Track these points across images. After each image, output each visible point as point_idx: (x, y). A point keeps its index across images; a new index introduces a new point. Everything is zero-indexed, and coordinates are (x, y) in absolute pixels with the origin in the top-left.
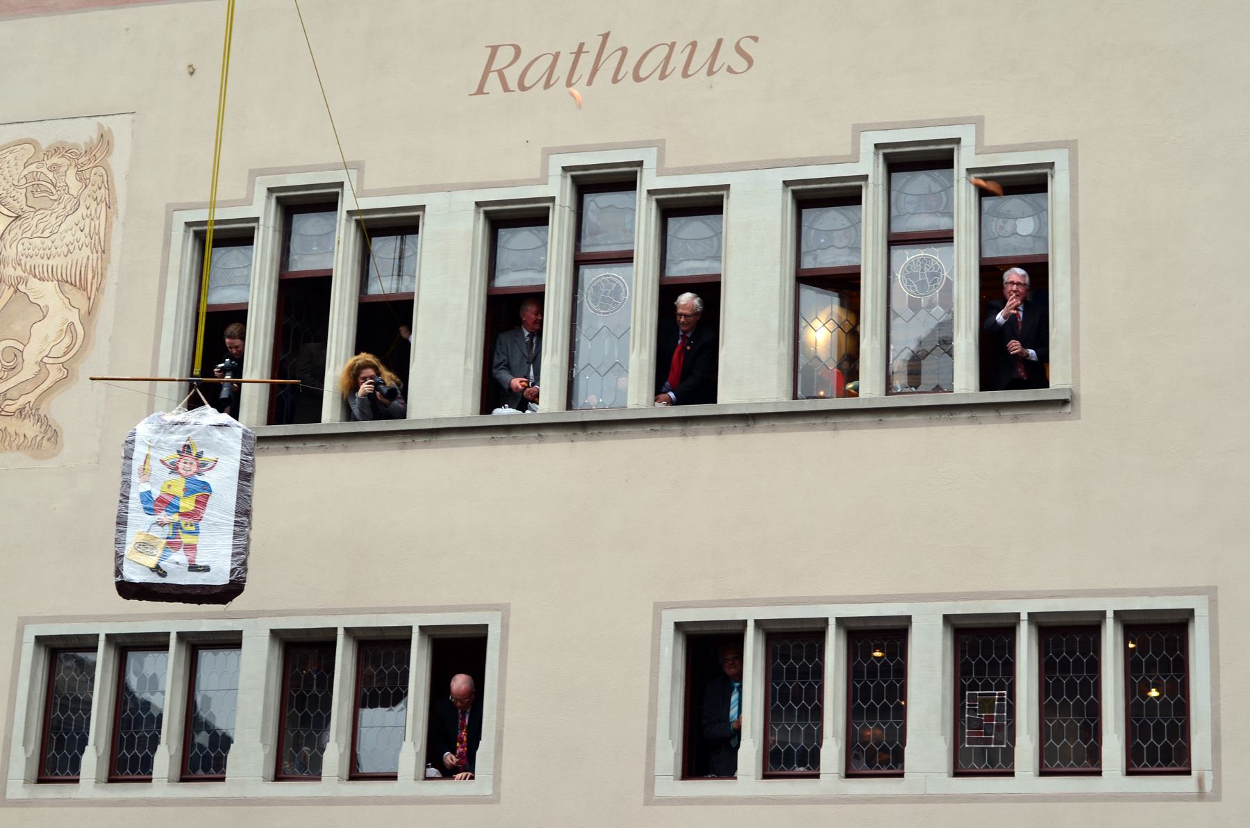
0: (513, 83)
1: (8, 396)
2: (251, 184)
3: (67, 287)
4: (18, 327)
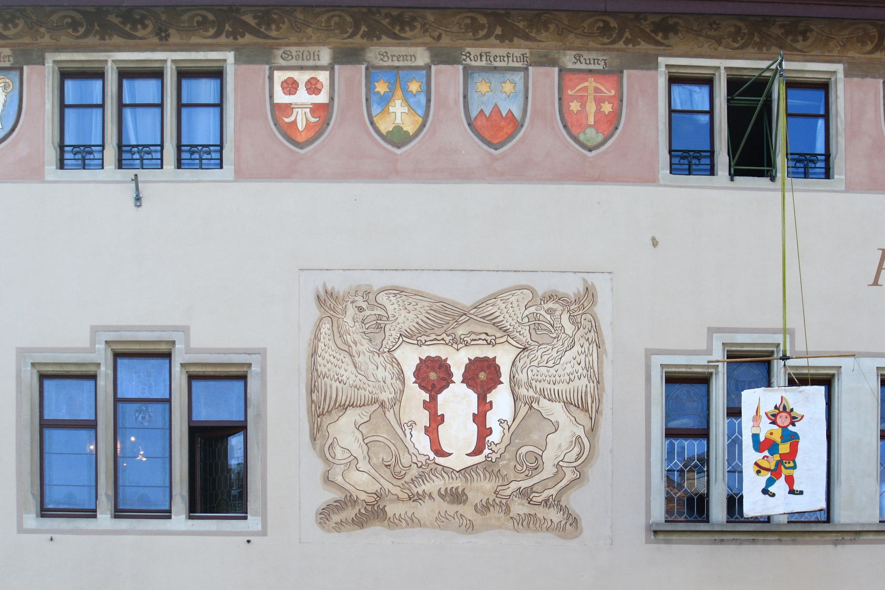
1: (534, 489)
3: (572, 408)
4: (535, 436)
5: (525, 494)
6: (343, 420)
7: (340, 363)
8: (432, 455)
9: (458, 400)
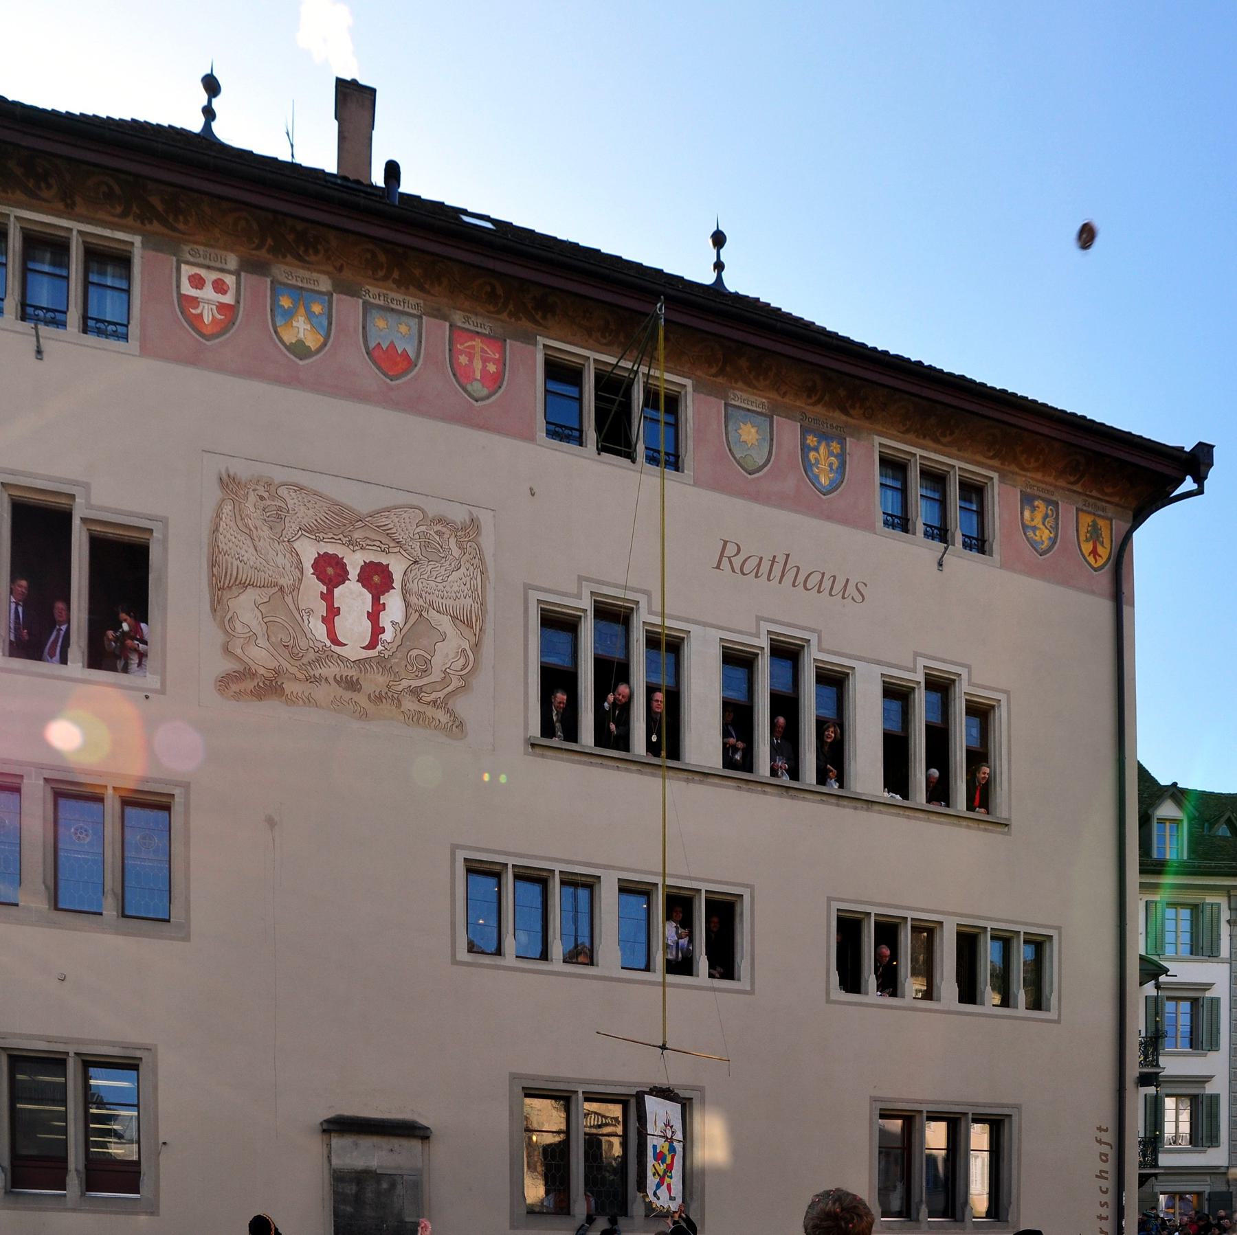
0: (738, 570)
2: (580, 587)
5: (416, 692)
6: (243, 597)
8: (328, 643)
9: (353, 598)
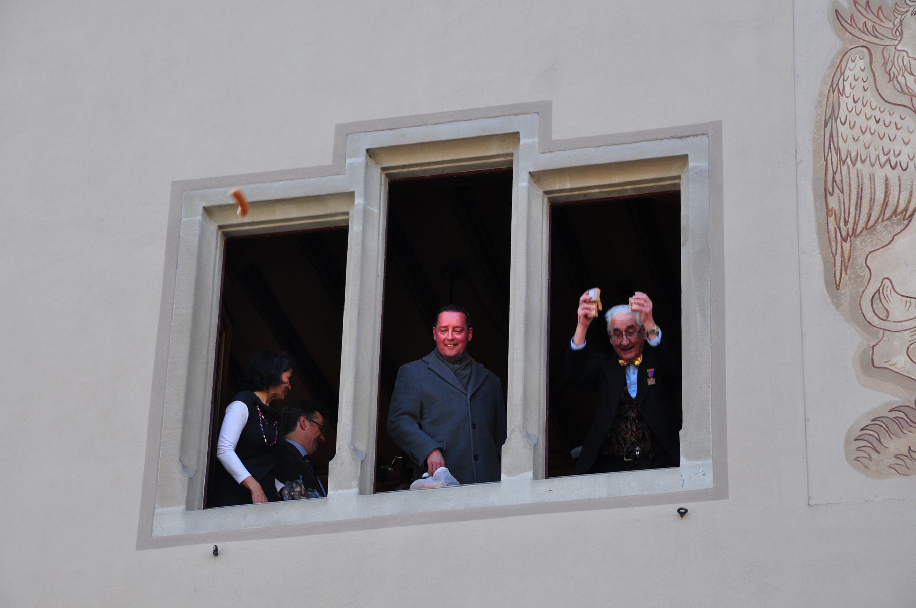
6: (902, 242)
7: (892, 131)
